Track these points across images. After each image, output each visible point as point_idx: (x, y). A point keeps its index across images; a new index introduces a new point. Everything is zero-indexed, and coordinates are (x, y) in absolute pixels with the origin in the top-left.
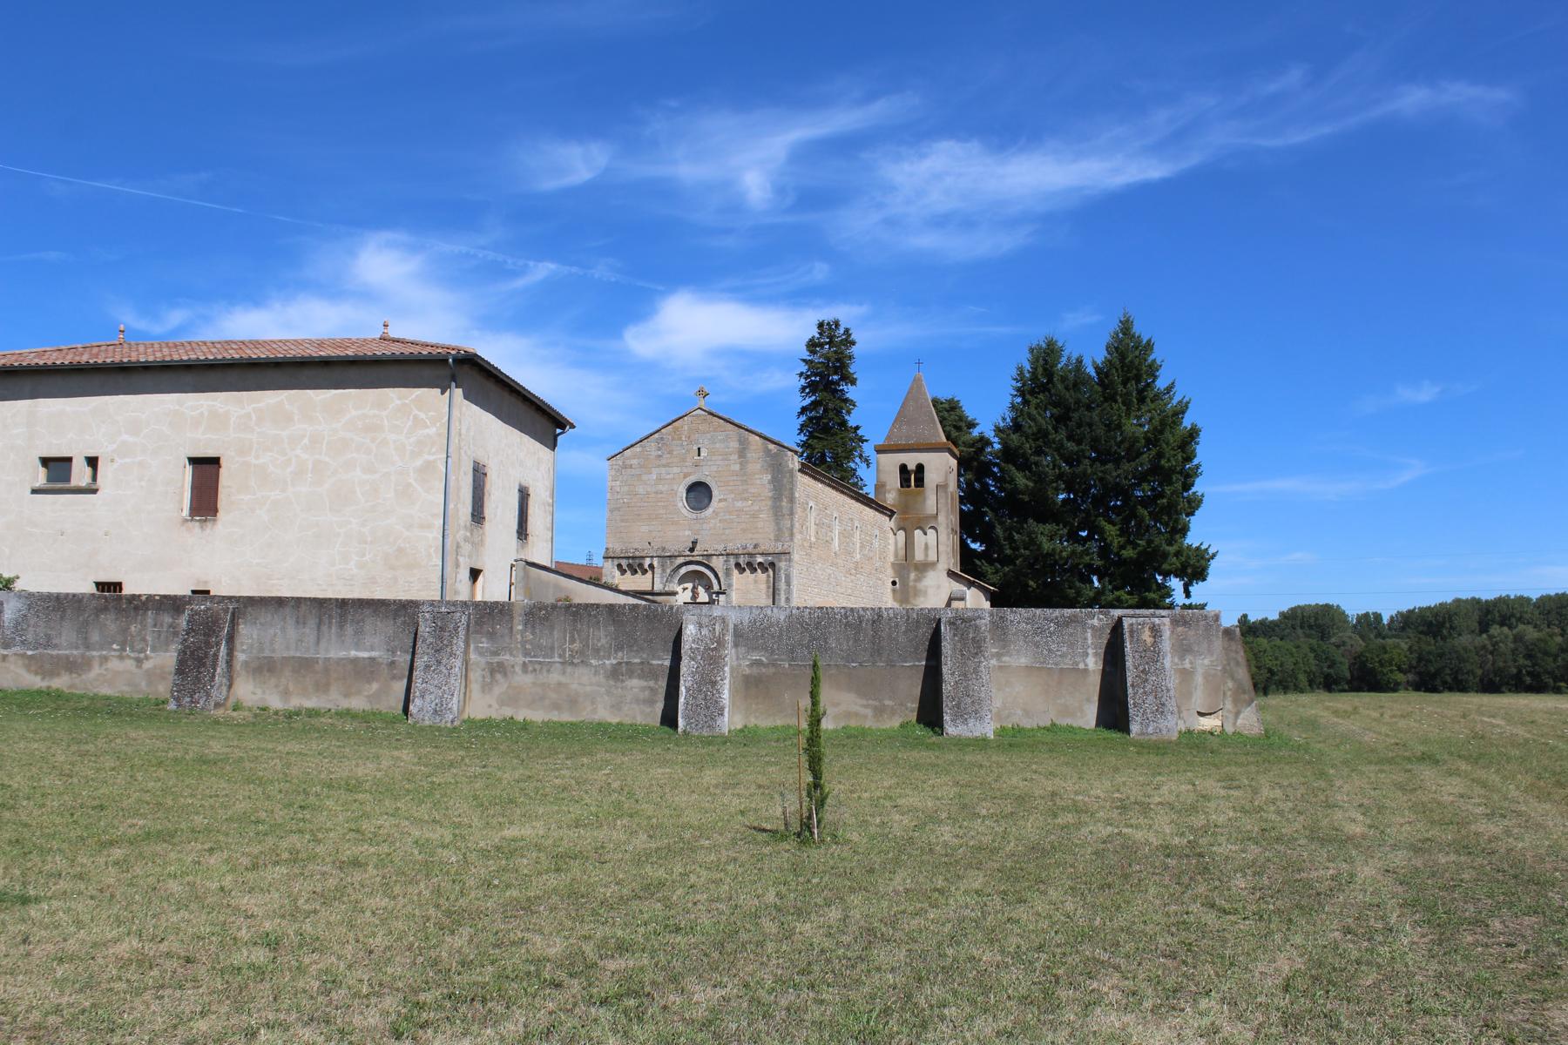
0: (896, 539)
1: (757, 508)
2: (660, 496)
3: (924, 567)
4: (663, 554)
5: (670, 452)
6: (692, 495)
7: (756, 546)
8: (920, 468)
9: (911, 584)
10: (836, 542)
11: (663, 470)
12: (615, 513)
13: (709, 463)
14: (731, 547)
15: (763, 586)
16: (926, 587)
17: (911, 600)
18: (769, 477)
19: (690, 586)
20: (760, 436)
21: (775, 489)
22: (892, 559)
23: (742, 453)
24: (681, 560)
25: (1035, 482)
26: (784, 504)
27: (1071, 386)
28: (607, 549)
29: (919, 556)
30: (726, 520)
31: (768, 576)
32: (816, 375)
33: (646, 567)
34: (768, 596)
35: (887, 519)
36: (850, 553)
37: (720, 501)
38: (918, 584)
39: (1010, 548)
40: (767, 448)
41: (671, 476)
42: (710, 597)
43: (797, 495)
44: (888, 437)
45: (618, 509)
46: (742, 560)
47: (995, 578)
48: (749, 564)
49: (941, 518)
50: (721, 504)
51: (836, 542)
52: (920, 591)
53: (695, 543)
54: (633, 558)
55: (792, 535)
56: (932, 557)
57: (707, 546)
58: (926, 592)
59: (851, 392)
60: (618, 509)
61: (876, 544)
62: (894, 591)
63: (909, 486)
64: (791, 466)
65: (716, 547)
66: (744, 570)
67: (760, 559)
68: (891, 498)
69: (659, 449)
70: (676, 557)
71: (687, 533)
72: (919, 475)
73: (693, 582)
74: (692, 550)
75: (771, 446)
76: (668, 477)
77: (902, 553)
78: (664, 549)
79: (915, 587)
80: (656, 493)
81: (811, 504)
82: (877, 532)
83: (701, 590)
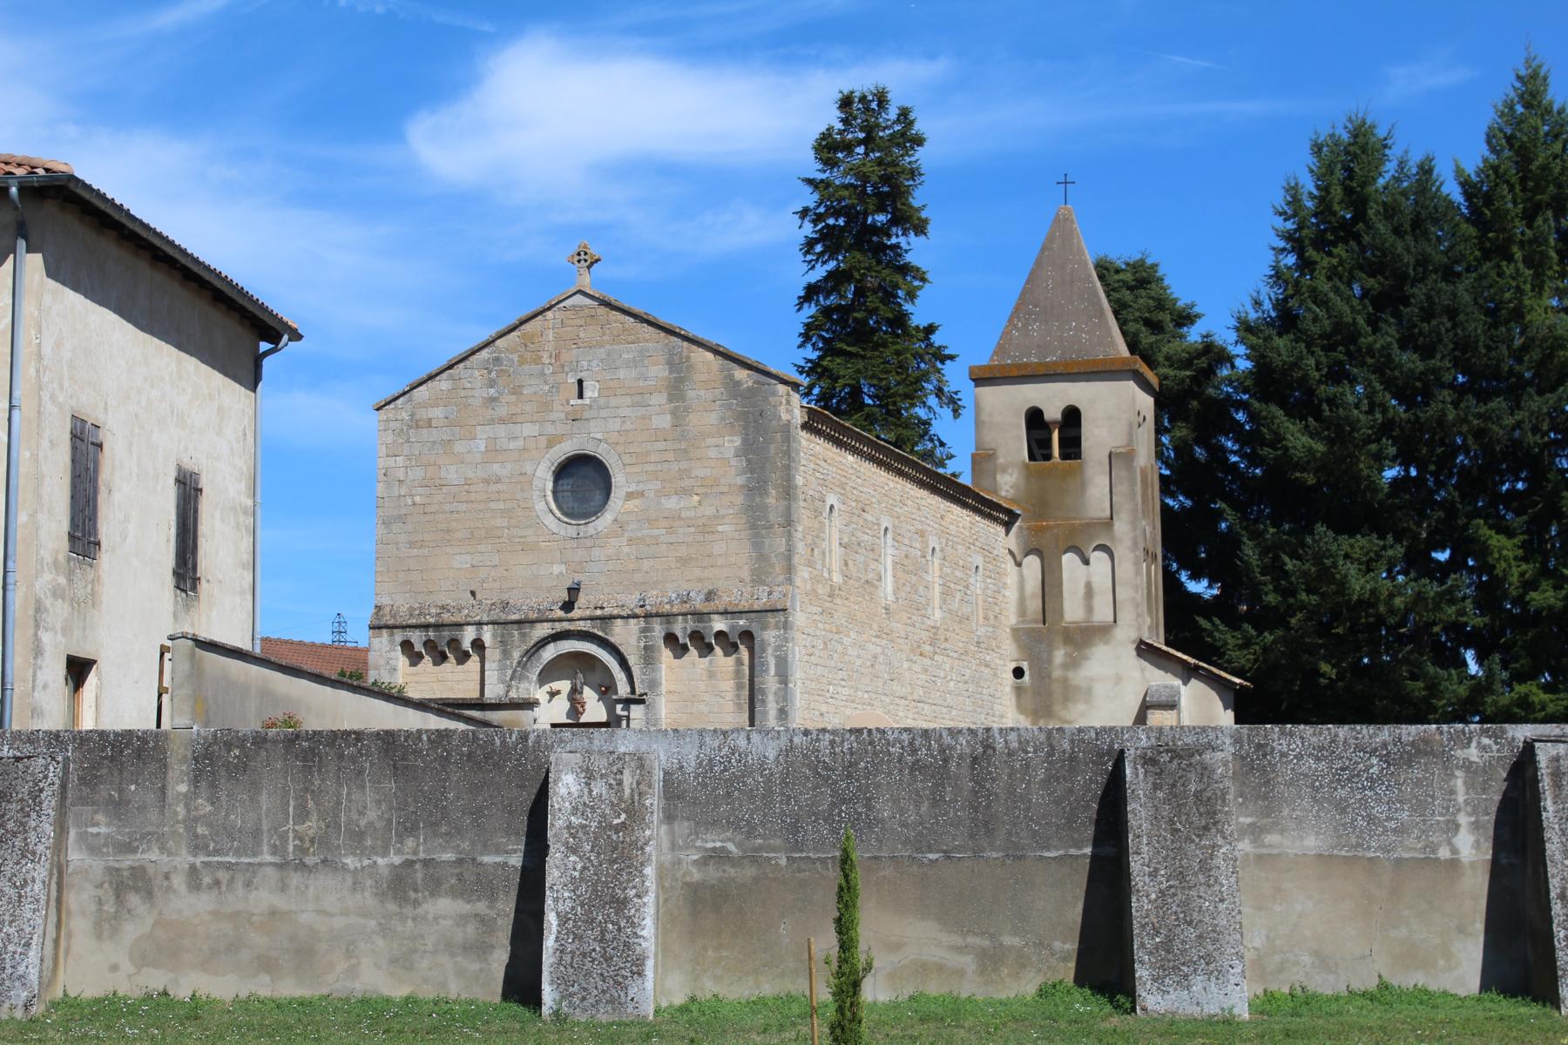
1: (709, 511)
2: (493, 488)
3: (1085, 636)
4: (503, 617)
5: (517, 391)
6: (566, 484)
7: (710, 596)
8: (1072, 416)
9: (1057, 674)
10: (889, 584)
11: (501, 431)
12: (394, 527)
13: (604, 413)
14: (654, 599)
15: (728, 686)
17: (1057, 708)
18: (737, 441)
19: (564, 686)
20: (716, 351)
22: (1012, 619)
23: (676, 388)
24: (543, 630)
25: (1331, 442)
27: (1407, 227)
28: (379, 608)
29: (1073, 611)
31: (739, 662)
32: (837, 214)
33: (466, 645)
34: (739, 706)
35: (1001, 530)
36: (920, 608)
38: (1071, 675)
39: (1276, 590)
40: (731, 377)
41: (519, 443)
42: (611, 710)
43: (799, 481)
44: (1000, 350)
45: (402, 518)
46: (680, 628)
47: (1243, 658)
48: (696, 637)
49: (1121, 526)
50: (633, 504)
51: (889, 584)
52: (1078, 688)
53: (574, 591)
54: (438, 626)
55: (789, 569)
56: (1103, 613)
57: (601, 599)
58: (1087, 694)
59: (916, 249)
60: (402, 518)
61: (977, 585)
62: (1019, 690)
63: (1048, 457)
64: (785, 417)
66: (685, 649)
67: (719, 625)
68: (1007, 485)
69: (492, 384)
70: (533, 622)
71: (558, 569)
73: (572, 677)
74: (568, 606)
75: (741, 374)
76: (512, 445)
77: (1034, 605)
78: (505, 605)
79: (1065, 680)
80: (486, 481)
81: (831, 499)
82: (978, 560)
83: (589, 695)
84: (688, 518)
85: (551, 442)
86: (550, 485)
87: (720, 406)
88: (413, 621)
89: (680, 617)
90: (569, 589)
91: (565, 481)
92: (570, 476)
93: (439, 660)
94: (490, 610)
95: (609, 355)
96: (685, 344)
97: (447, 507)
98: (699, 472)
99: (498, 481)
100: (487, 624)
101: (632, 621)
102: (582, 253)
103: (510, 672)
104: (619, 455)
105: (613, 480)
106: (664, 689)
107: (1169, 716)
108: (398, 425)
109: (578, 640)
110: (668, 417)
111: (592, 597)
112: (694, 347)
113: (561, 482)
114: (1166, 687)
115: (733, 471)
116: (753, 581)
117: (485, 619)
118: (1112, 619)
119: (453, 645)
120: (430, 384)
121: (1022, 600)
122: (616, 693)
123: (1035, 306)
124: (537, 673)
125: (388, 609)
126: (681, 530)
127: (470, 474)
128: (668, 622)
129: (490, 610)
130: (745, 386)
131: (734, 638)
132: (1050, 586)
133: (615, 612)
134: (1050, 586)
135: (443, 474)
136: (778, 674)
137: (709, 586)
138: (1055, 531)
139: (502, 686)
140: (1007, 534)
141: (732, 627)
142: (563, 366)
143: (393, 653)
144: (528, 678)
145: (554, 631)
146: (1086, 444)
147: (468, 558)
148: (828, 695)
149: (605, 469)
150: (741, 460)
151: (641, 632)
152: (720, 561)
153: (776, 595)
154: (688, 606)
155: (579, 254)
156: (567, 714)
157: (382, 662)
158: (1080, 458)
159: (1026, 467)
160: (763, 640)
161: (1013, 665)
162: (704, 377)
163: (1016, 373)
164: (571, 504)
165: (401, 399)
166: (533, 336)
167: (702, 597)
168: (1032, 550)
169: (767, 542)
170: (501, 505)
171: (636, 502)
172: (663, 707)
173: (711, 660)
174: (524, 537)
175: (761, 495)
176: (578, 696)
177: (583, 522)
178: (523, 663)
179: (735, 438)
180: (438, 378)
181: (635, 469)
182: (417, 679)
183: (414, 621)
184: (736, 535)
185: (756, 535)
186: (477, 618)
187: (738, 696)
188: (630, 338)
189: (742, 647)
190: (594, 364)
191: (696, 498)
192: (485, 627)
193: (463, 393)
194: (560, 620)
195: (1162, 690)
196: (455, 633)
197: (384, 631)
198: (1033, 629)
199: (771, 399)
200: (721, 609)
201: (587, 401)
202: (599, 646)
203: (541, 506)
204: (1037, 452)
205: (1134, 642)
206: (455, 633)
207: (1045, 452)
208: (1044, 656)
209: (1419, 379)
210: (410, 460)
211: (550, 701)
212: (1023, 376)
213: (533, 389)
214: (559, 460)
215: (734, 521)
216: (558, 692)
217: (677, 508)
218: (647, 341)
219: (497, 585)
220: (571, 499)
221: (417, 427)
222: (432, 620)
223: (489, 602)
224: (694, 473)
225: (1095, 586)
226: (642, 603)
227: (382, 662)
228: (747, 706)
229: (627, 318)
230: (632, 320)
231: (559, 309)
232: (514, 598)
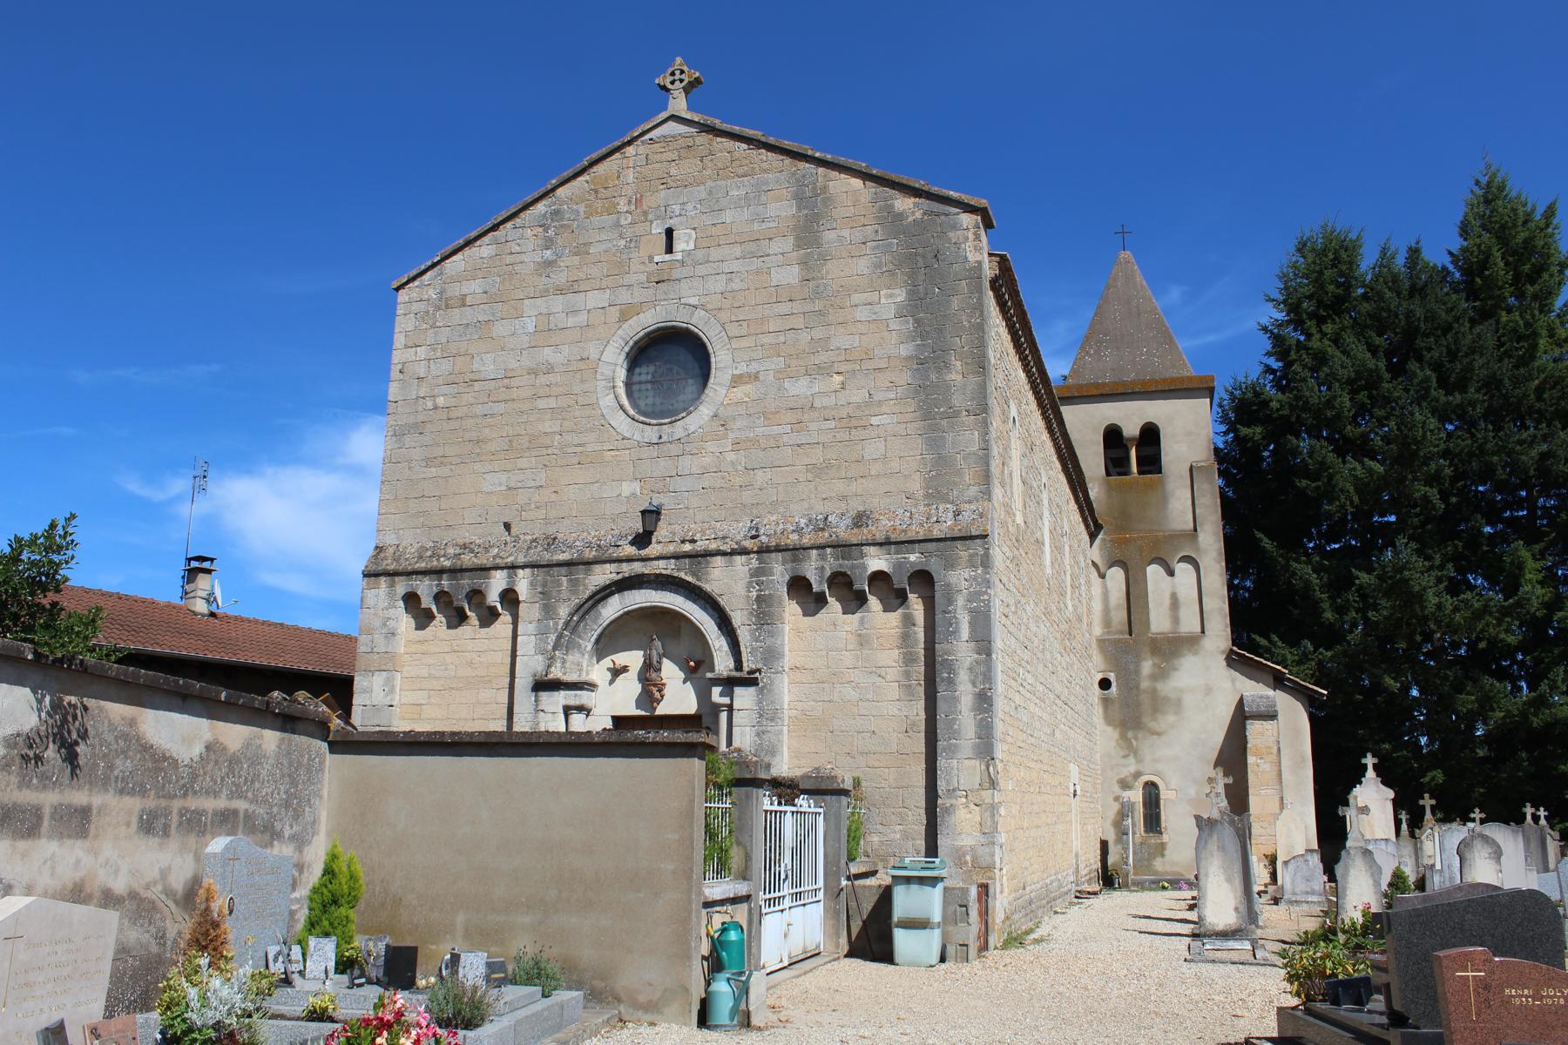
0: (1105, 587)
1: (859, 396)
2: (542, 379)
3: (1172, 647)
5: (581, 250)
6: (645, 373)
7: (860, 520)
8: (1150, 434)
11: (558, 304)
12: (407, 440)
13: (701, 270)
14: (772, 527)
15: (889, 658)
16: (1181, 691)
17: (1145, 719)
18: (901, 295)
19: (633, 659)
20: (865, 176)
21: (921, 332)
22: (1098, 630)
23: (808, 232)
24: (603, 575)
26: (954, 376)
28: (379, 549)
29: (1159, 622)
30: (755, 442)
31: (908, 621)
33: (493, 598)
35: (1087, 538)
37: (737, 380)
38: (1159, 686)
40: (889, 209)
41: (582, 318)
42: (703, 696)
45: (418, 428)
46: (814, 570)
50: (739, 393)
52: (1167, 699)
53: (652, 515)
54: (455, 572)
56: (1190, 624)
57: (693, 529)
58: (1178, 704)
60: (418, 428)
62: (1106, 701)
63: (1127, 473)
65: (723, 528)
66: (821, 600)
67: (877, 562)
69: (548, 244)
70: (589, 563)
71: (628, 488)
72: (1148, 451)
73: (646, 646)
74: (642, 540)
75: (904, 203)
76: (571, 321)
77: (1120, 616)
78: (551, 542)
79: (1154, 692)
80: (533, 372)
83: (671, 672)
84: (825, 408)
85: (623, 318)
86: (622, 374)
87: (878, 247)
88: (422, 565)
89: (814, 552)
90: (643, 513)
91: (644, 369)
92: (650, 361)
93: (455, 620)
94: (529, 548)
95: (710, 193)
96: (821, 170)
97: (479, 410)
98: (841, 340)
99: (550, 370)
100: (523, 567)
101: (738, 559)
102: (677, 72)
103: (553, 637)
104: (723, 325)
105: (713, 360)
106: (788, 661)
107: (1270, 727)
108: (422, 306)
109: (656, 589)
110: (796, 269)
111: (677, 528)
112: (834, 174)
113: (637, 370)
114: (1261, 697)
115: (894, 337)
116: (927, 496)
117: (521, 560)
118: (1199, 630)
119: (475, 600)
120: (467, 251)
121: (1106, 610)
122: (713, 670)
123: (1105, 335)
124: (593, 639)
125: (391, 550)
126: (813, 426)
127: (513, 364)
128: (795, 560)
129: (529, 548)
130: (911, 219)
131: (901, 581)
132: (1135, 597)
133: (713, 546)
134: (1135, 597)
135: (476, 366)
136: (973, 638)
137: (856, 506)
138: (1139, 543)
139: (540, 658)
140: (1091, 546)
141: (898, 566)
142: (645, 213)
143: (392, 611)
145: (620, 576)
146: (1164, 459)
147: (503, 477)
148: (1020, 681)
149: (703, 346)
150: (907, 322)
151: (752, 576)
152: (875, 469)
153: (966, 516)
154: (827, 535)
155: (673, 74)
156: (637, 701)
157: (377, 623)
158: (1160, 472)
159: (1108, 483)
160: (948, 585)
161: (1100, 676)
162: (850, 211)
163: (1095, 392)
164: (650, 401)
165: (429, 273)
166: (606, 181)
167: (849, 521)
168: (1116, 562)
169: (950, 437)
170: (552, 403)
171: (747, 388)
172: (786, 691)
173: (862, 619)
174: (580, 445)
175: (939, 370)
176: (654, 675)
177: (667, 421)
178: (573, 624)
179: (897, 291)
180: (478, 243)
181: (745, 343)
182: (424, 648)
183: (423, 565)
184: (900, 429)
185: (934, 428)
186: (510, 559)
187: (907, 675)
188: (740, 171)
189: (912, 597)
190: (689, 207)
191: (838, 378)
192: (520, 572)
193: (509, 259)
194: (629, 560)
195: (1258, 700)
196: (478, 582)
197: (383, 579)
198: (1119, 641)
199: (951, 235)
200: (880, 537)
201: (679, 256)
202: (687, 597)
203: (607, 401)
204: (1111, 469)
205: (1223, 652)
206: (478, 582)
207: (1118, 470)
208: (1132, 667)
209: (1453, 412)
210: (434, 350)
211: (611, 682)
212: (1102, 395)
213: (603, 247)
214: (635, 338)
215: (897, 409)
216: (625, 669)
217: (809, 393)
218: (765, 171)
219: (541, 514)
220: (651, 393)
221: (447, 307)
222: (447, 564)
223: (529, 537)
224: (834, 344)
225: (1181, 597)
226: (754, 533)
227: (377, 623)
228: (921, 690)
229: (737, 144)
230: (744, 146)
231: (642, 142)
232: (564, 531)
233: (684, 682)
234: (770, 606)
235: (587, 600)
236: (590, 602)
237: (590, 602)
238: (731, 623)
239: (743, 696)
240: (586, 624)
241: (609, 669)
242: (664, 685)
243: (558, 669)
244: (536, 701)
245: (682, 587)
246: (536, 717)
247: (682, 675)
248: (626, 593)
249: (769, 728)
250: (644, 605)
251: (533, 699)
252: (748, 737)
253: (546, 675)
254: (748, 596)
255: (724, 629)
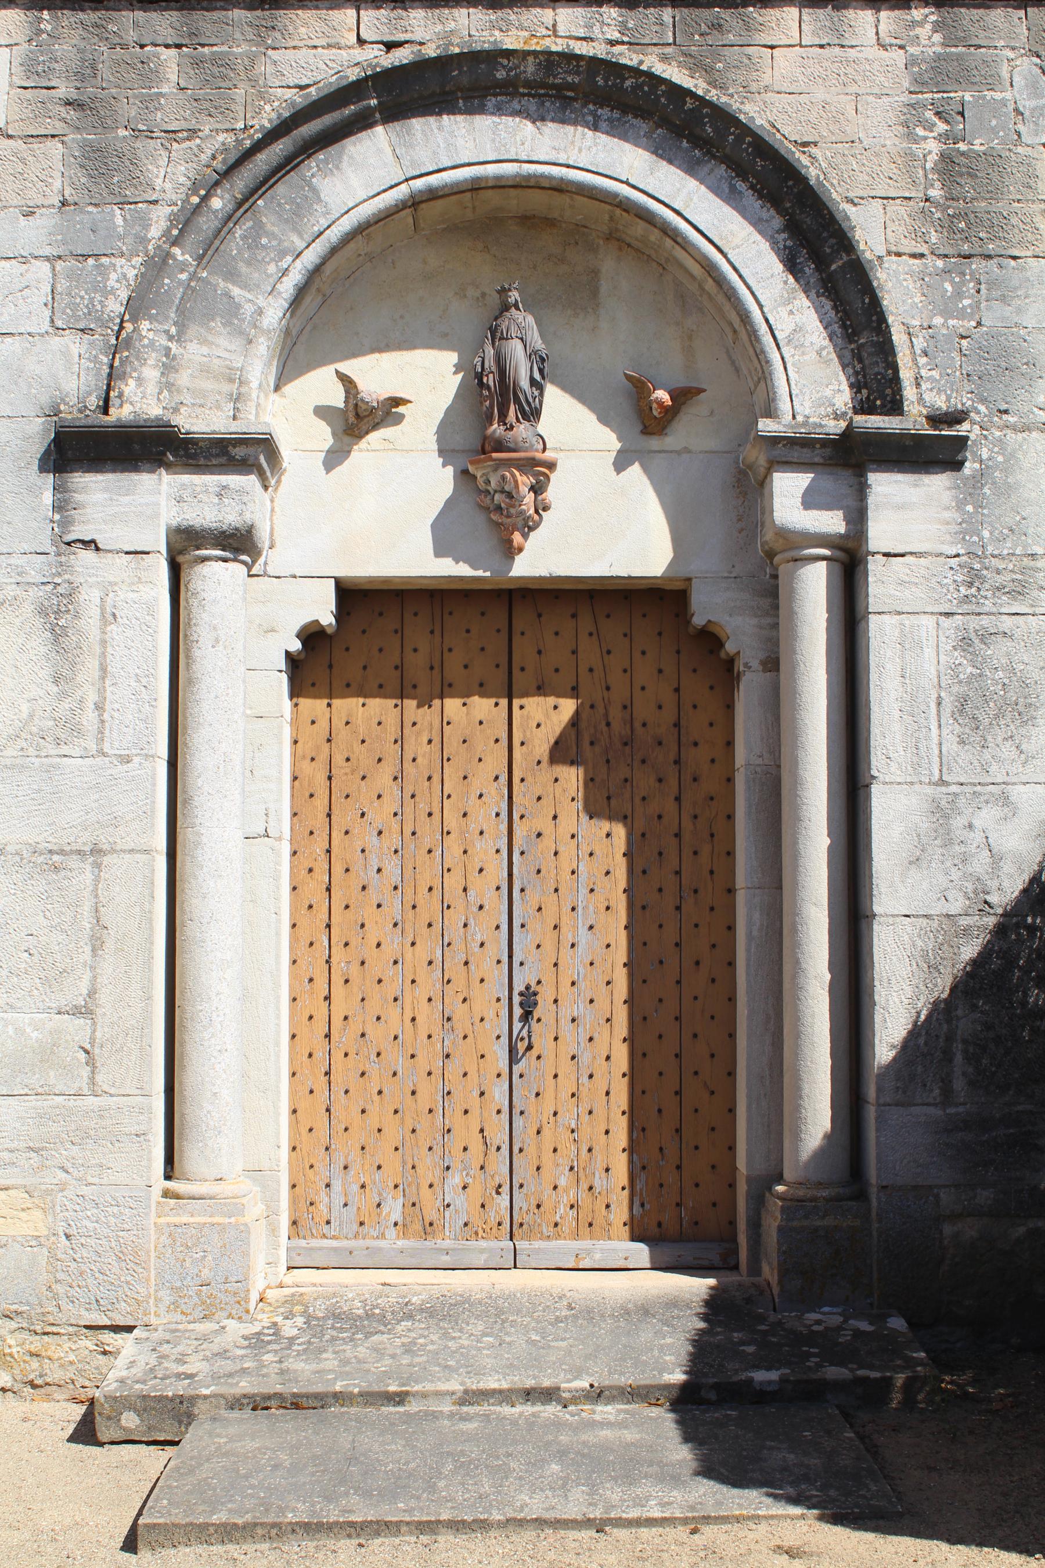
109: (537, 118)
122: (770, 412)
124: (288, 287)
139: (74, 345)
144: (233, 309)
145: (402, 56)
151: (920, 84)
156: (437, 527)
178: (206, 224)
202: (660, 151)
211: (334, 458)
233: (620, 464)
234: (995, 194)
235: (273, 135)
236: (280, 148)
237: (280, 148)
238: (844, 242)
239: (901, 507)
240: (259, 226)
241: (322, 412)
242: (551, 466)
243: (152, 388)
244: (59, 507)
245: (642, 113)
246: (63, 568)
247: (610, 441)
248: (417, 124)
249: (1007, 623)
250: (491, 170)
251: (48, 498)
252: (929, 652)
253: (106, 412)
254: (910, 155)
255: (809, 269)
